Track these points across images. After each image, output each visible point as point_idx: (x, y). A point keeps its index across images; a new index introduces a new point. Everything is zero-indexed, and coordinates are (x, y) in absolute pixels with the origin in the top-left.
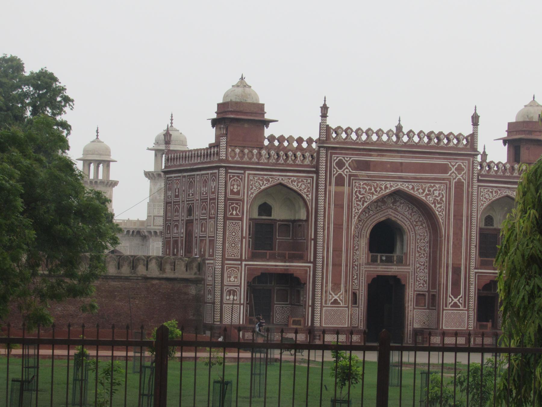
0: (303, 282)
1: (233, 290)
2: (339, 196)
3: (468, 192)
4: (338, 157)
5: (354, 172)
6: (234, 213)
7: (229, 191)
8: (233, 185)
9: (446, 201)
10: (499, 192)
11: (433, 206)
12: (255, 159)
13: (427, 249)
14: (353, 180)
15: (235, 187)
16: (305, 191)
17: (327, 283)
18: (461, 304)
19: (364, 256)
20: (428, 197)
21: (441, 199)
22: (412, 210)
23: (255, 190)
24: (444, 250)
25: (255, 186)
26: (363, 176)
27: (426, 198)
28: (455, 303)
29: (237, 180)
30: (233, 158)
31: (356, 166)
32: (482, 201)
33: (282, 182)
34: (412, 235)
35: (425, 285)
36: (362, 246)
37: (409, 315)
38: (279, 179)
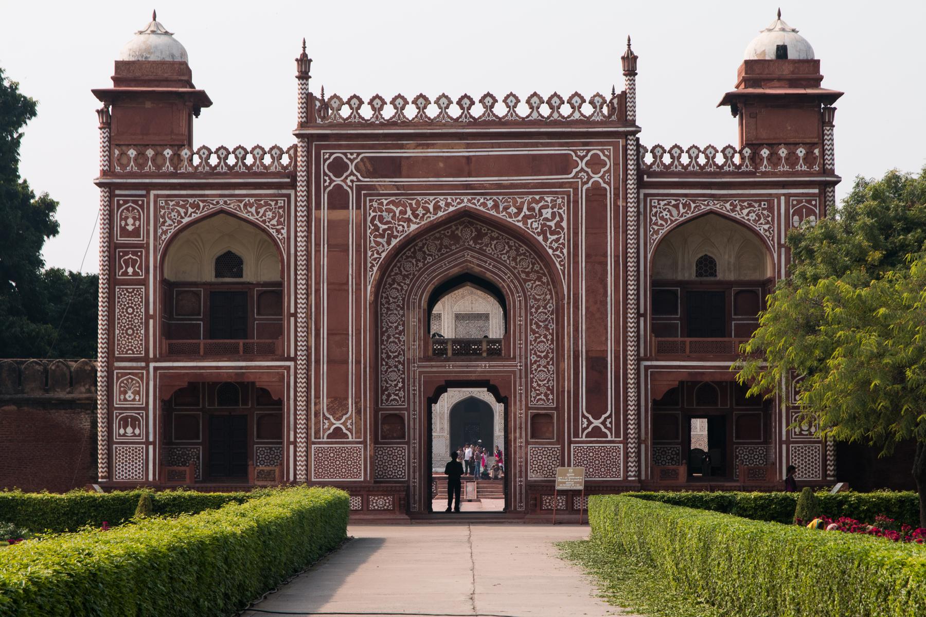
0: (275, 398)
1: (131, 417)
2: (337, 228)
3: (617, 207)
4: (331, 154)
5: (367, 181)
6: (130, 270)
7: (117, 230)
8: (127, 218)
9: (569, 229)
10: (693, 205)
11: (540, 238)
12: (168, 167)
15: (130, 221)
16: (274, 222)
17: (317, 397)
18: (610, 429)
20: (529, 221)
21: (558, 225)
22: (517, 250)
23: (170, 225)
25: (170, 218)
26: (386, 187)
27: (525, 223)
28: (597, 428)
29: (134, 209)
30: (123, 167)
32: (656, 224)
33: (225, 207)
35: (551, 397)
36: (411, 324)
37: (518, 456)
38: (218, 203)
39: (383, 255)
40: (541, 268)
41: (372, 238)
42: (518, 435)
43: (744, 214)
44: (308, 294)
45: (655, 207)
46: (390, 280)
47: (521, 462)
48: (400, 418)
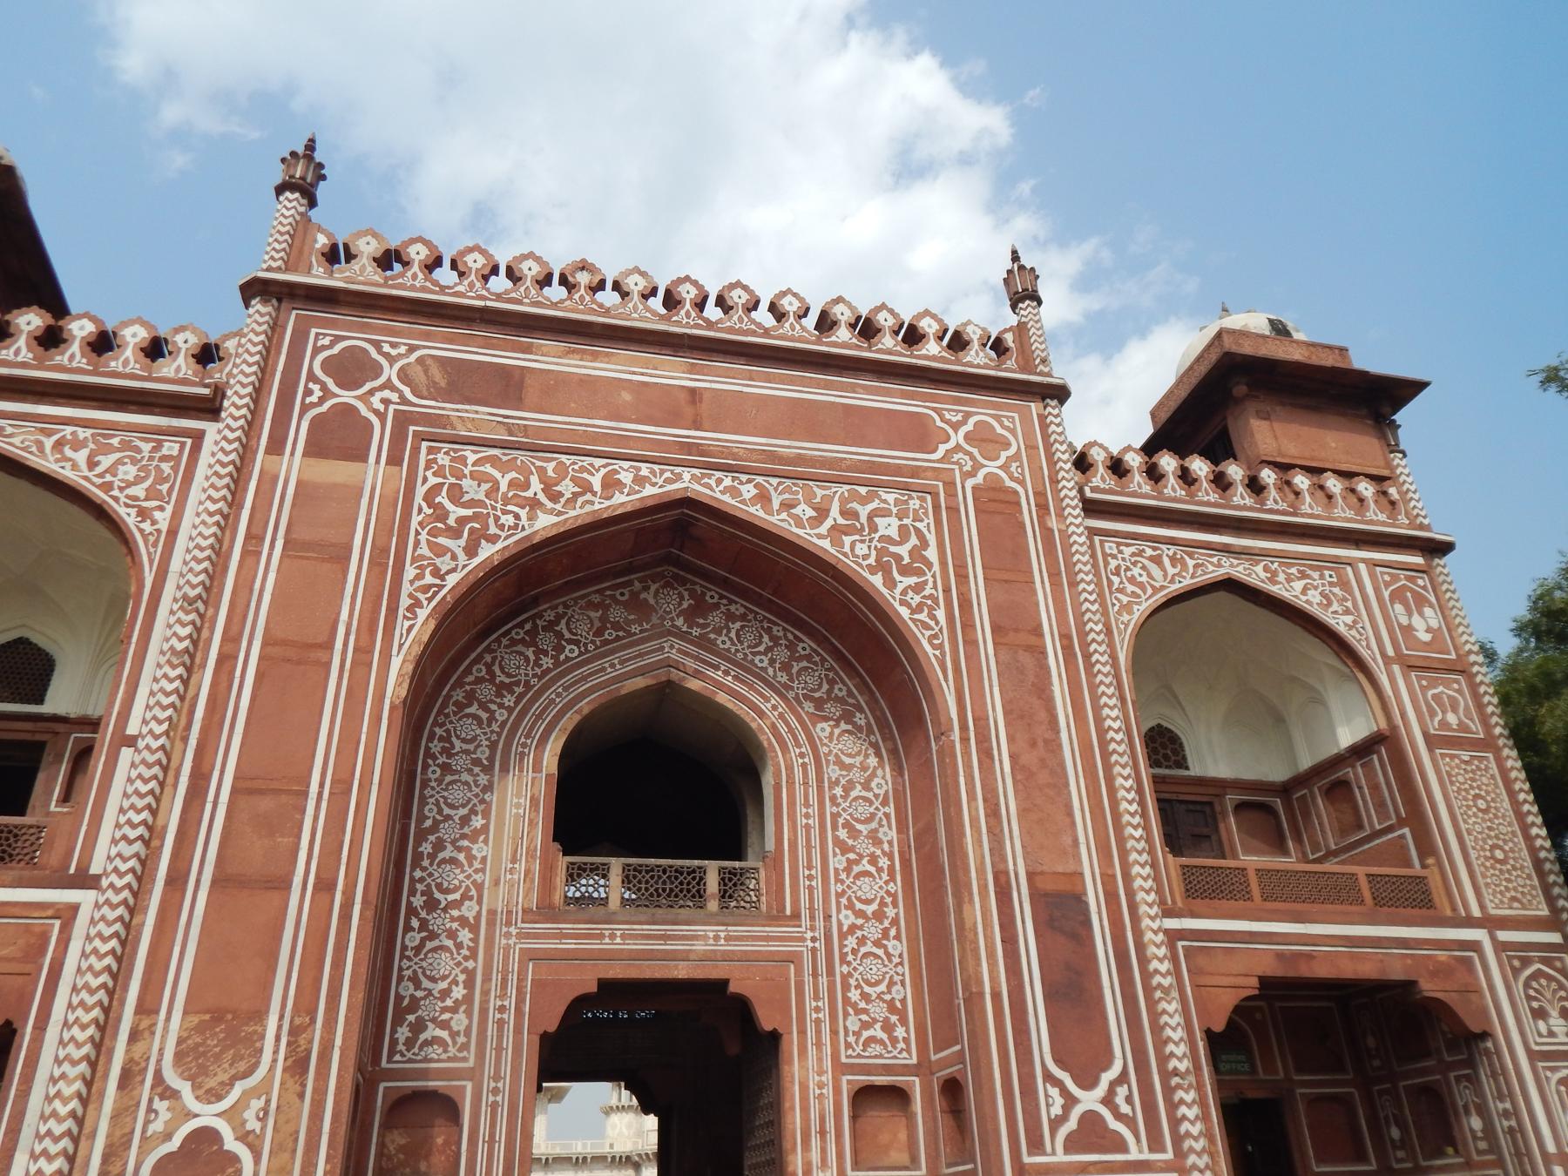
3: (1047, 534)
5: (430, 406)
9: (943, 563)
10: (1191, 563)
11: (877, 580)
13: (890, 834)
16: (139, 491)
17: (147, 1008)
18: (1129, 1121)
19: (521, 866)
20: (847, 540)
22: (791, 647)
31: (443, 384)
32: (1120, 590)
35: (900, 1032)
36: (510, 812)
39: (452, 580)
41: (424, 536)
42: (815, 1156)
43: (1291, 590)
45: (1114, 557)
46: (459, 695)
48: (448, 1107)
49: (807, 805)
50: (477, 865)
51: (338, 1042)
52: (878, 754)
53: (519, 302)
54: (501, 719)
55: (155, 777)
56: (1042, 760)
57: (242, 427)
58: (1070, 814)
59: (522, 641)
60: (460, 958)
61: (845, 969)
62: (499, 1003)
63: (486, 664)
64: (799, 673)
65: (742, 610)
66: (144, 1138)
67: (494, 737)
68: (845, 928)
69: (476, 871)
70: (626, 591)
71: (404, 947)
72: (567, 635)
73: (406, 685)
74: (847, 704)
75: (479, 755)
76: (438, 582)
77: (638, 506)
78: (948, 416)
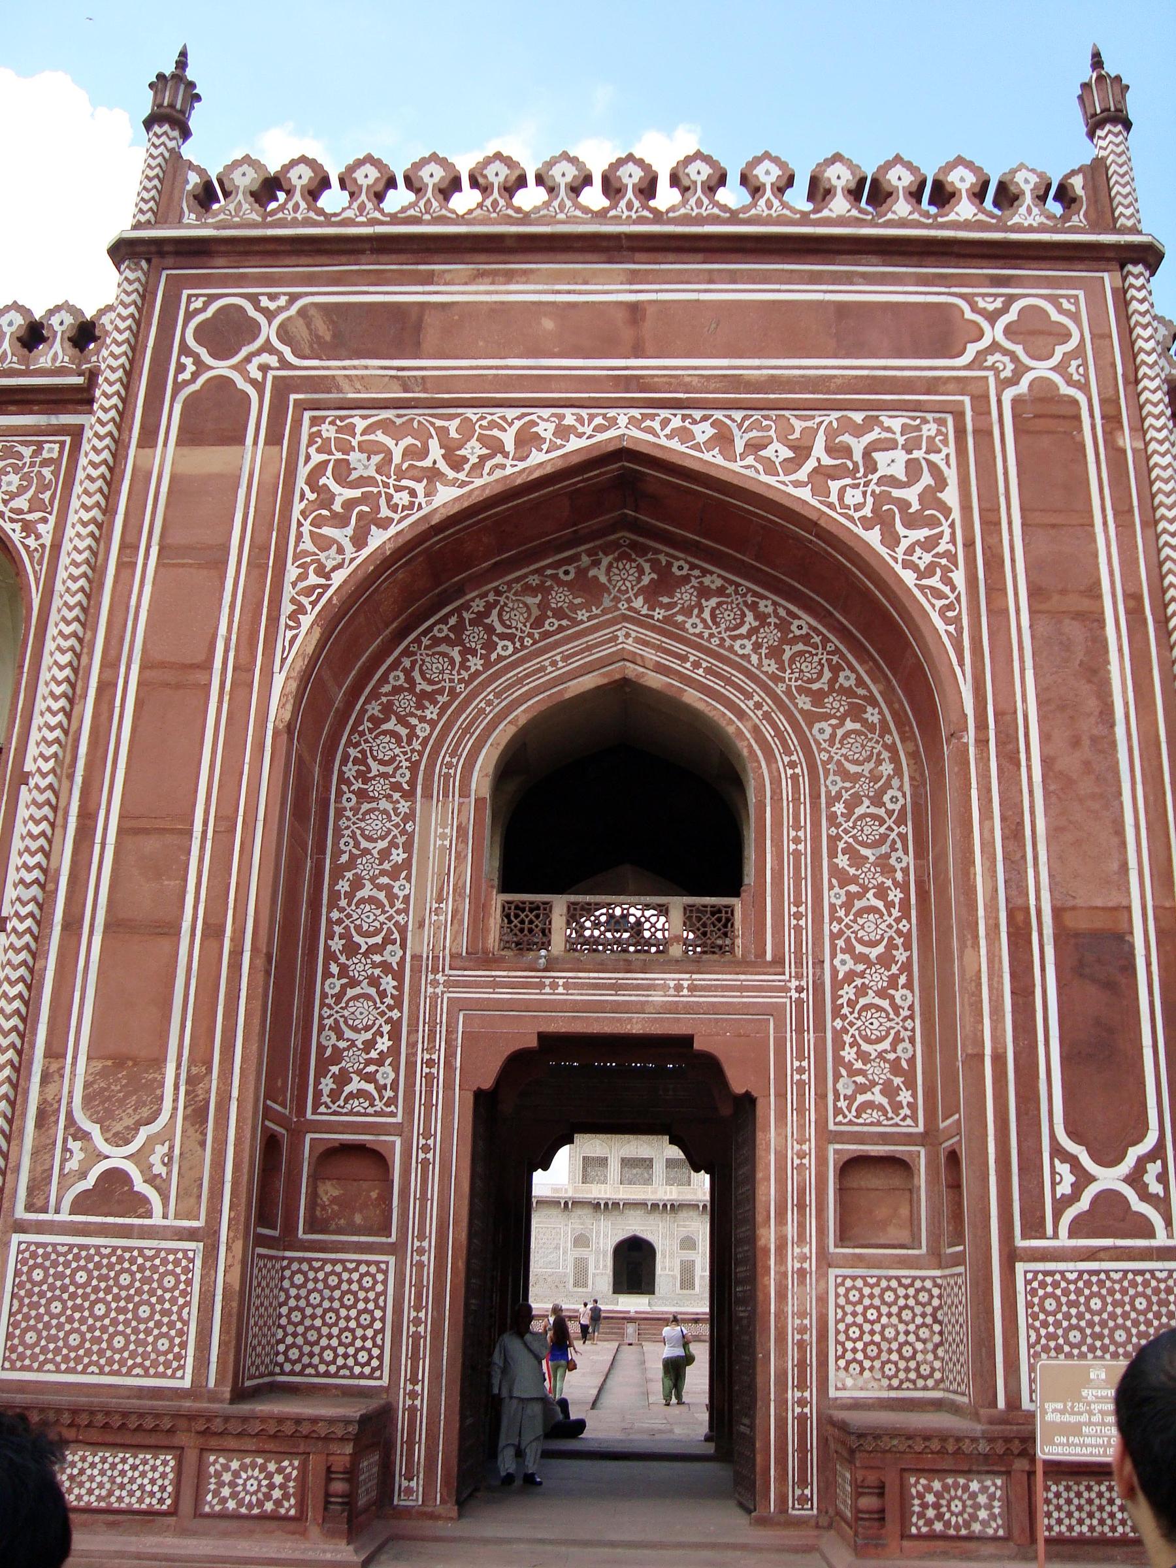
3: (1116, 456)
4: (212, 298)
5: (314, 367)
9: (966, 508)
11: (873, 537)
14: (301, 406)
16: (22, 503)
17: (55, 1052)
20: (835, 486)
21: (930, 497)
22: (783, 626)
24: (986, 813)
26: (366, 382)
31: (328, 338)
34: (786, 774)
35: (905, 1096)
36: (435, 843)
39: (338, 578)
40: (860, 682)
41: (306, 528)
42: (791, 1230)
44: (73, 700)
46: (374, 709)
47: (802, 1330)
48: (377, 1159)
49: (797, 827)
50: (399, 905)
51: (235, 1093)
52: (895, 759)
53: (417, 221)
54: (422, 735)
55: (46, 818)
56: (1087, 764)
57: (113, 420)
58: (1120, 832)
59: (446, 640)
60: (383, 1007)
61: (838, 1024)
62: (427, 1056)
63: (404, 670)
64: (792, 660)
65: (719, 582)
66: (62, 1175)
67: (415, 757)
68: (841, 976)
69: (398, 912)
70: (572, 569)
71: (324, 995)
72: (500, 629)
73: (289, 707)
74: (856, 696)
75: (398, 778)
76: (323, 581)
77: (560, 465)
78: (981, 304)
